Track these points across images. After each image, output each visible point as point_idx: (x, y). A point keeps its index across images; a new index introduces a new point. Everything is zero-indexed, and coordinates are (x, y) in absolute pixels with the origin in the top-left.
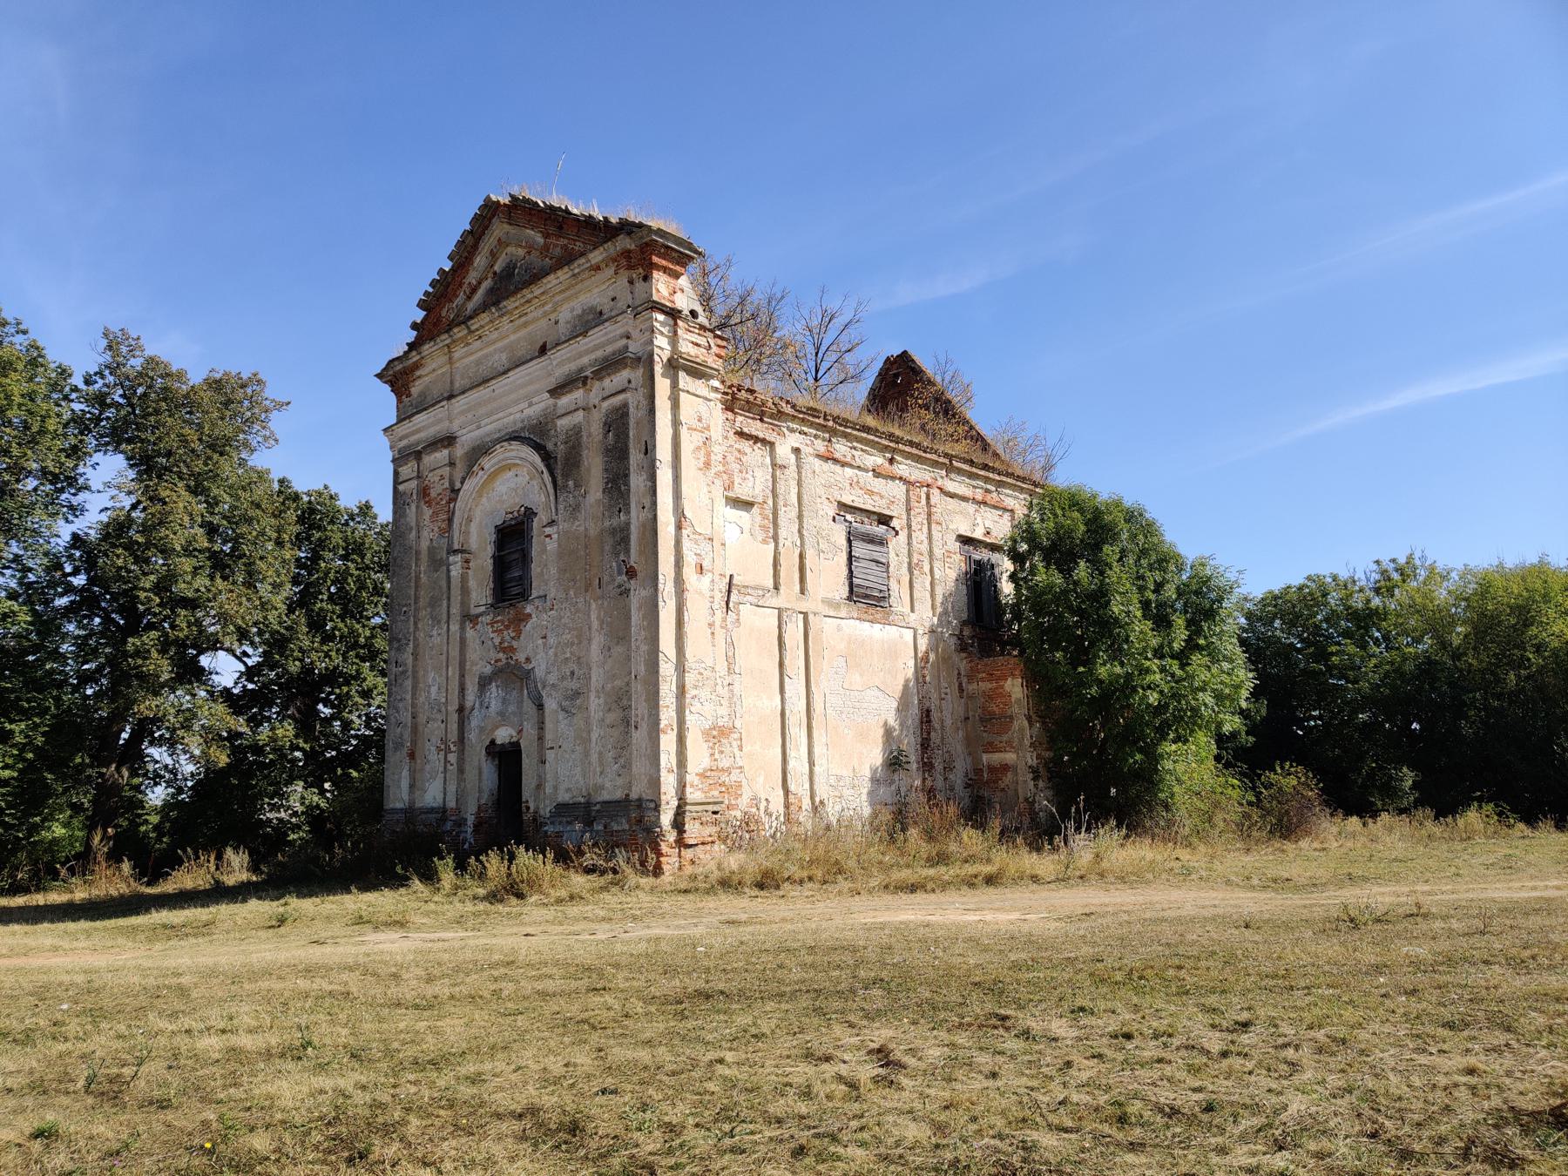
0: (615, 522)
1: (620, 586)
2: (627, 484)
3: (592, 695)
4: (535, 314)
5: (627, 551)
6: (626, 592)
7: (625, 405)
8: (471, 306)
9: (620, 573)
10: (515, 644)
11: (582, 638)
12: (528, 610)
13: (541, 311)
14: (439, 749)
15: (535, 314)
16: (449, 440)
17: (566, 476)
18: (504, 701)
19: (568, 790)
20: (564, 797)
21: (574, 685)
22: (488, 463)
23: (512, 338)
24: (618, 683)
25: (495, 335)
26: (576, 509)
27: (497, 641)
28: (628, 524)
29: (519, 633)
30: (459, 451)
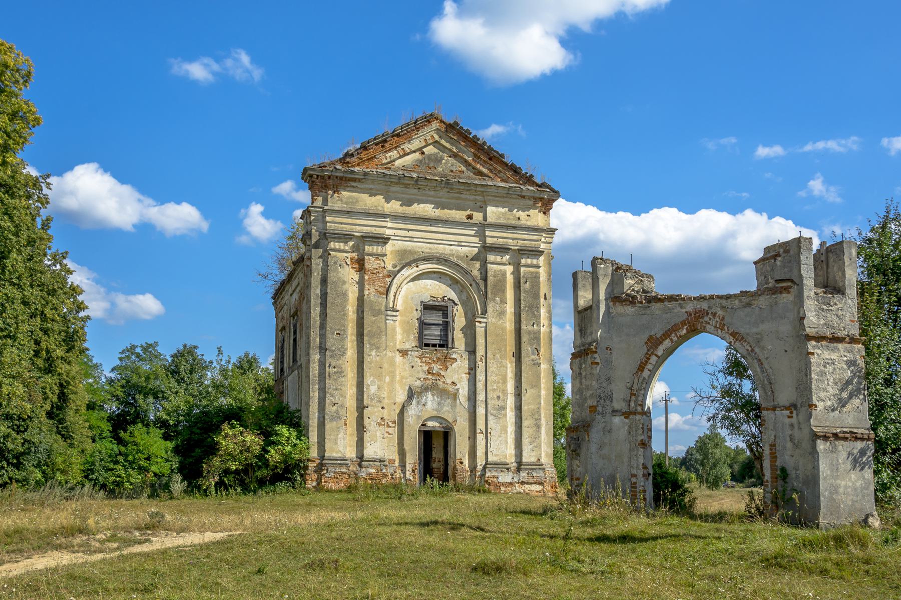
0: (530, 328)
1: (533, 360)
2: (539, 312)
3: (508, 410)
4: (468, 197)
5: (539, 344)
6: (539, 365)
7: (538, 273)
8: (398, 163)
9: (533, 354)
10: (443, 373)
11: (505, 381)
12: (454, 356)
13: (472, 197)
14: (380, 425)
15: (468, 197)
16: (384, 240)
17: (495, 295)
18: (439, 404)
19: (496, 455)
20: (491, 459)
21: (500, 403)
22: (425, 267)
23: (443, 200)
24: (532, 407)
25: (432, 193)
26: (502, 313)
27: (426, 368)
28: (539, 332)
29: (447, 368)
30: (389, 247)
